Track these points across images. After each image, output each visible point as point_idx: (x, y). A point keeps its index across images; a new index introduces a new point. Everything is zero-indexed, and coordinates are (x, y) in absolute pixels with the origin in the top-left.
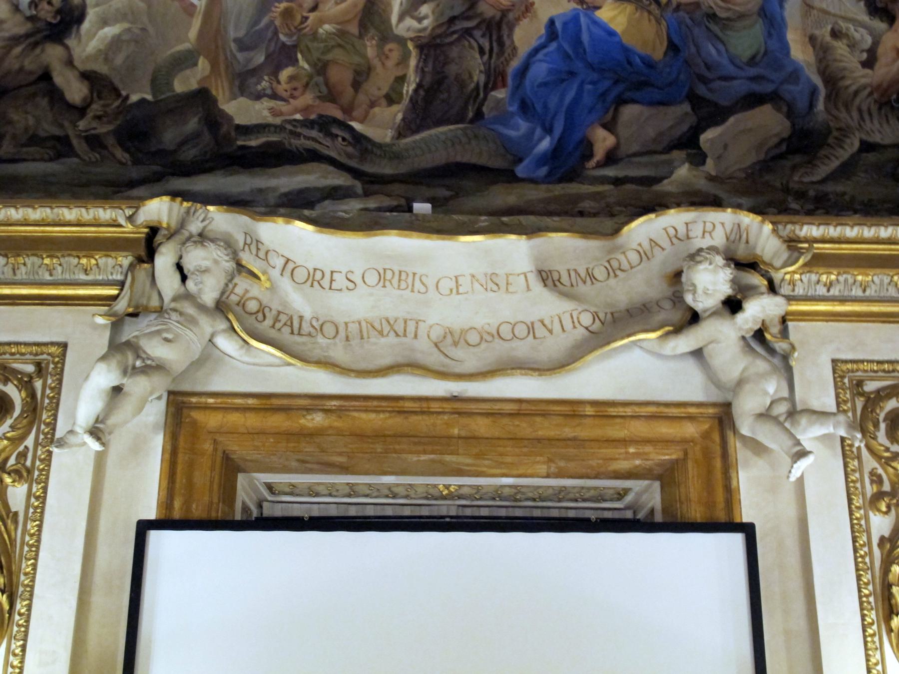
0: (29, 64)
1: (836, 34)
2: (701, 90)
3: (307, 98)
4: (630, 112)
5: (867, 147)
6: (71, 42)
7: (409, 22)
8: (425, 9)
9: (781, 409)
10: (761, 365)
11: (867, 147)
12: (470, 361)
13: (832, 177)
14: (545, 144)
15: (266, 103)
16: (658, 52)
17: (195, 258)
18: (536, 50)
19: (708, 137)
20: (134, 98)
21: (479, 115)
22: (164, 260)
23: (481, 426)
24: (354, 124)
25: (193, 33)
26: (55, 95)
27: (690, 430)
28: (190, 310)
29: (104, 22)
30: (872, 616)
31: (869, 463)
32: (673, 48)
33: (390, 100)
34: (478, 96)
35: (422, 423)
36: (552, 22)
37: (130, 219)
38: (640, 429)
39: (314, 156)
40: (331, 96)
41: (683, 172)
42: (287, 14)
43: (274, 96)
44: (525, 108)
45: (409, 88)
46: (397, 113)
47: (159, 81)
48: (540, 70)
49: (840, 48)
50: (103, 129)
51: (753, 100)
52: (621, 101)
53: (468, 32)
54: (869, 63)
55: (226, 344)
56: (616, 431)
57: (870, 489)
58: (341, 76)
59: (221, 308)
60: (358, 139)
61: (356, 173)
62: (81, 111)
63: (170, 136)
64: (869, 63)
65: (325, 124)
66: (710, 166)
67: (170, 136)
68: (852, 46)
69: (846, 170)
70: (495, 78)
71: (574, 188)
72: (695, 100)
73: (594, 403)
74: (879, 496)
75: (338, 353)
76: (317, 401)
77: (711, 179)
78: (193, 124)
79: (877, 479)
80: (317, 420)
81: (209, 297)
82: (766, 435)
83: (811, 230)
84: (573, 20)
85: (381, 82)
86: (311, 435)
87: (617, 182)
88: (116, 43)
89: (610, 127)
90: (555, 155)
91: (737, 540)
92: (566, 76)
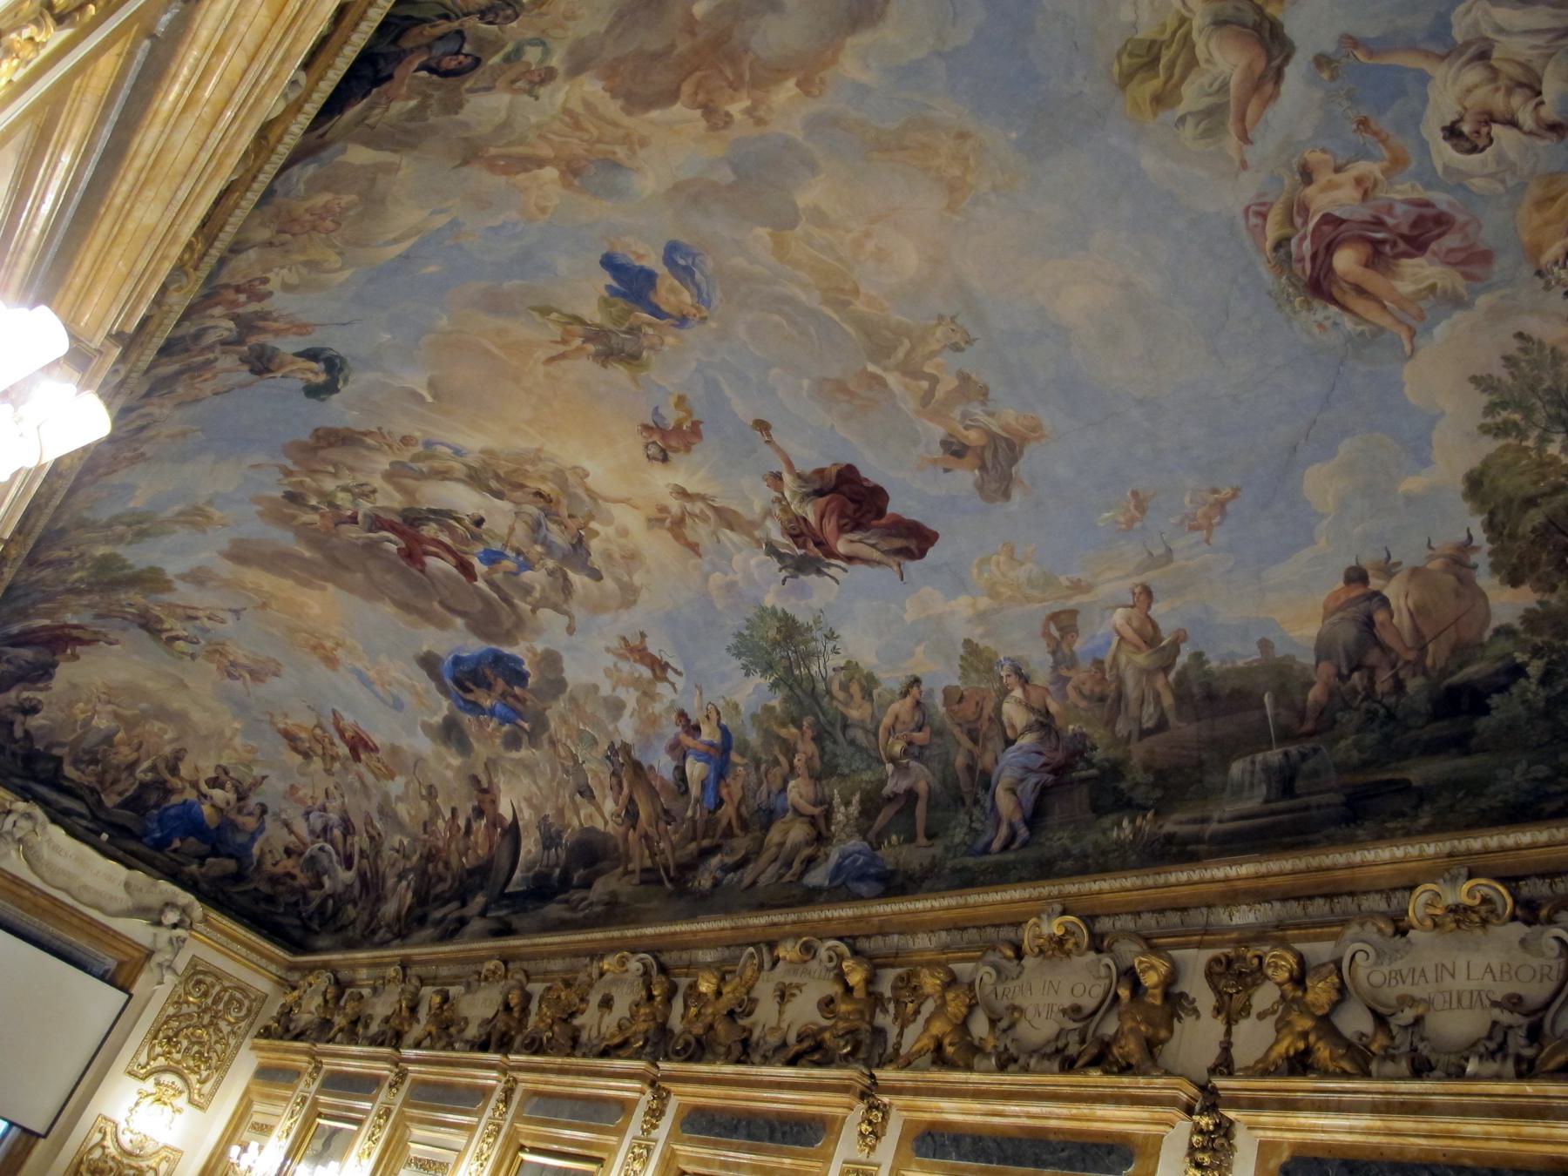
0: (10, 717)
1: (270, 851)
2: (218, 845)
3: (93, 779)
4: (192, 839)
5: (256, 889)
6: (29, 718)
7: (142, 775)
8: (150, 774)
9: (167, 964)
10: (169, 948)
11: (256, 889)
12: (86, 897)
13: (238, 893)
14: (158, 835)
15: (79, 773)
16: (213, 826)
17: (25, 824)
18: (173, 806)
19: (210, 860)
20: (37, 747)
21: (143, 815)
22: (11, 819)
23: (75, 921)
24: (103, 796)
25: (71, 738)
26: (11, 731)
27: (136, 954)
28: (9, 838)
29: (44, 718)
30: (149, 1036)
31: (182, 991)
32: (218, 828)
33: (120, 794)
34: (147, 809)
35: (58, 911)
36: (185, 801)
37: (11, 802)
38: (122, 947)
39: (80, 798)
40: (101, 782)
41: (193, 868)
42: (105, 751)
43: (83, 772)
44: (160, 821)
45: (127, 794)
46: (118, 800)
47: (51, 745)
48: (172, 812)
49: (268, 857)
50: (20, 751)
51: (231, 856)
52: (191, 835)
53: (158, 789)
54: (275, 865)
55: (13, 853)
56: (115, 944)
57: (176, 999)
58: (109, 778)
59: (20, 841)
60: (100, 802)
61: (91, 811)
62: (16, 741)
63: (40, 766)
64: (275, 865)
65: (93, 791)
66: (204, 870)
67: (40, 766)
68: (273, 857)
69: (245, 893)
70: (157, 806)
71: (158, 855)
72: (213, 847)
73: (115, 932)
74: (176, 1002)
75: (47, 875)
76: (30, 887)
77: (202, 875)
78: (51, 766)
79: (180, 996)
80: (26, 893)
81: (18, 836)
82: (156, 971)
83: (214, 915)
84: (192, 804)
85: (120, 787)
86: (21, 897)
87: (172, 859)
88: (42, 727)
89: (182, 840)
90: (160, 839)
91: (126, 996)
92: (178, 817)
